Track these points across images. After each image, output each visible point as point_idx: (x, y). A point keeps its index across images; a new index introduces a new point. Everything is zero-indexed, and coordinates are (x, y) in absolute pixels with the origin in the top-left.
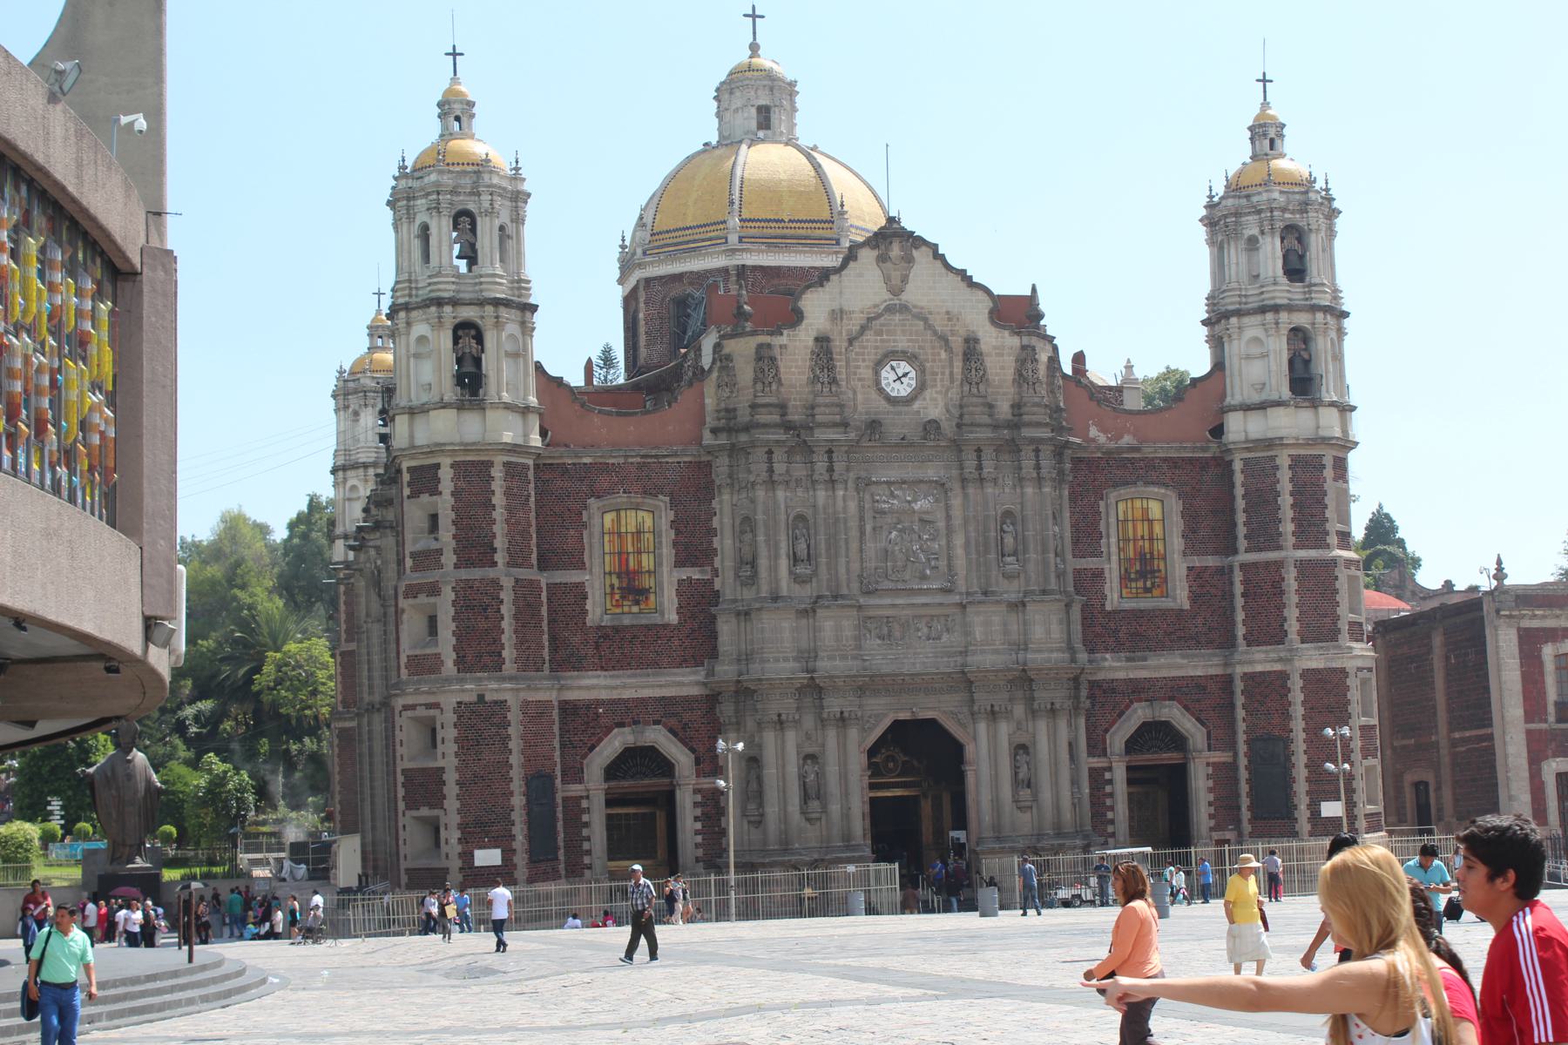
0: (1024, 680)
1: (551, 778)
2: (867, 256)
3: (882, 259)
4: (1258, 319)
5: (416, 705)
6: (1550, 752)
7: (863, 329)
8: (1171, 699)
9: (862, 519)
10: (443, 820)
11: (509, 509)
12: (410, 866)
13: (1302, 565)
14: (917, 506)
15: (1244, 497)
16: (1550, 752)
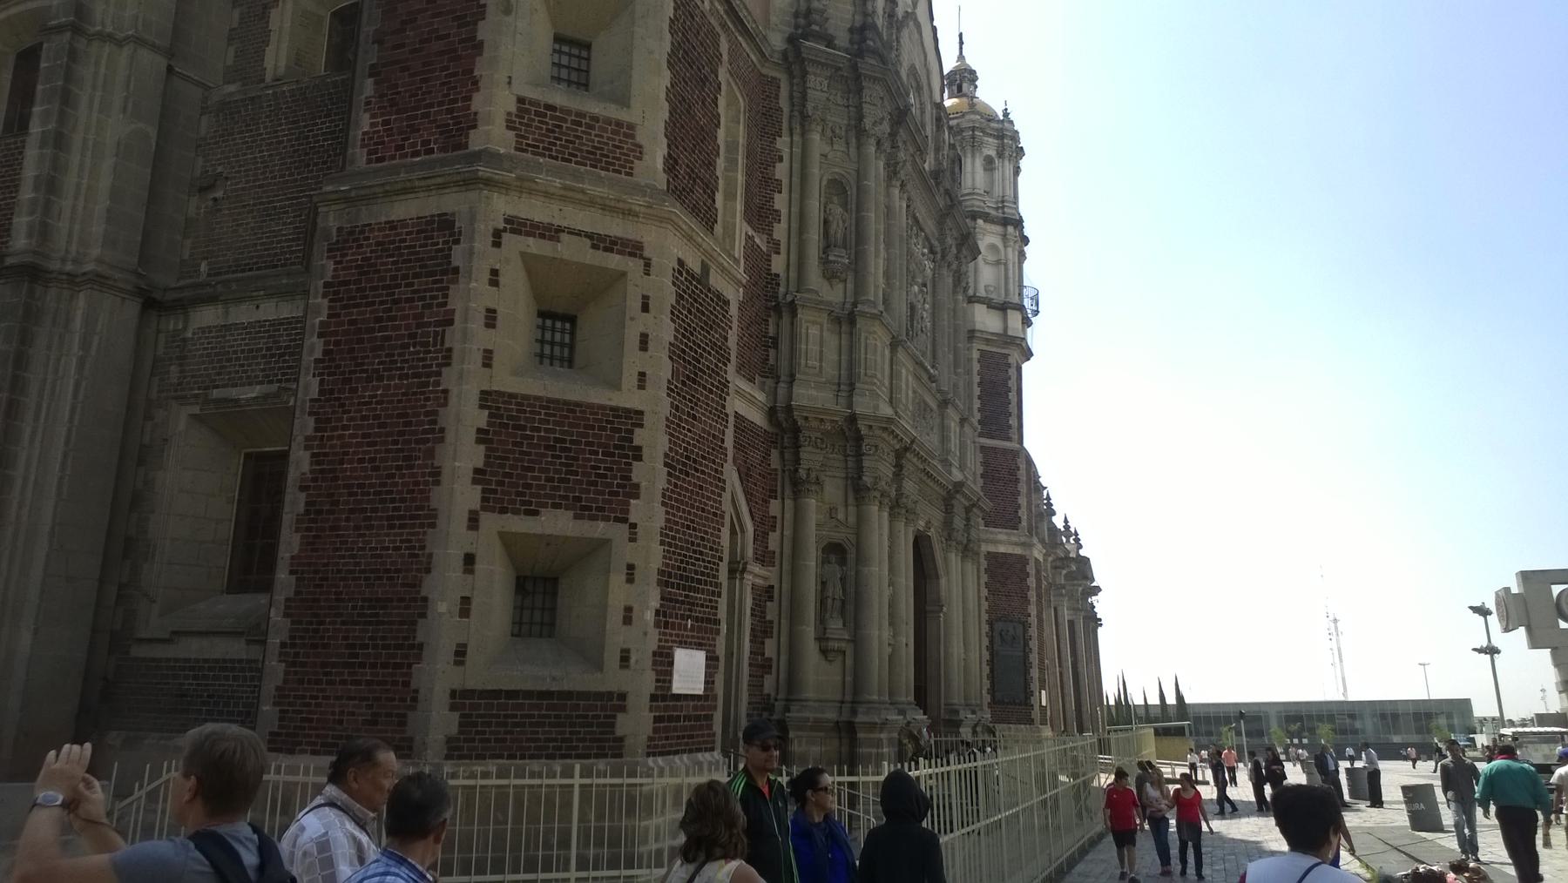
4: (999, 229)
5: (559, 230)
10: (624, 552)
12: (471, 684)
15: (980, 384)
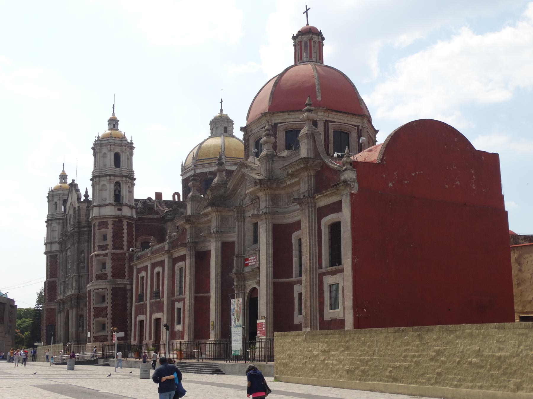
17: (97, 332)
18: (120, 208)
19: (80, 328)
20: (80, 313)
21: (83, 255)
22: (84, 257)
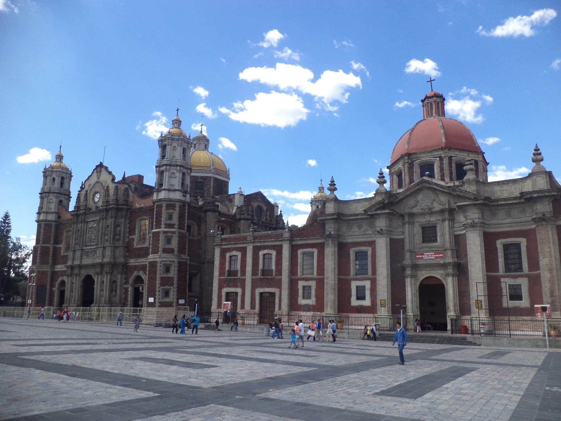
0: (102, 265)
1: (46, 287)
2: (95, 171)
3: (97, 172)
6: (225, 286)
7: (92, 188)
8: (141, 270)
9: (86, 230)
11: (45, 233)
13: (154, 233)
14: (94, 226)
16: (225, 286)
17: (162, 298)
18: (184, 194)
19: (113, 292)
20: (113, 279)
21: (118, 229)
22: (120, 231)
